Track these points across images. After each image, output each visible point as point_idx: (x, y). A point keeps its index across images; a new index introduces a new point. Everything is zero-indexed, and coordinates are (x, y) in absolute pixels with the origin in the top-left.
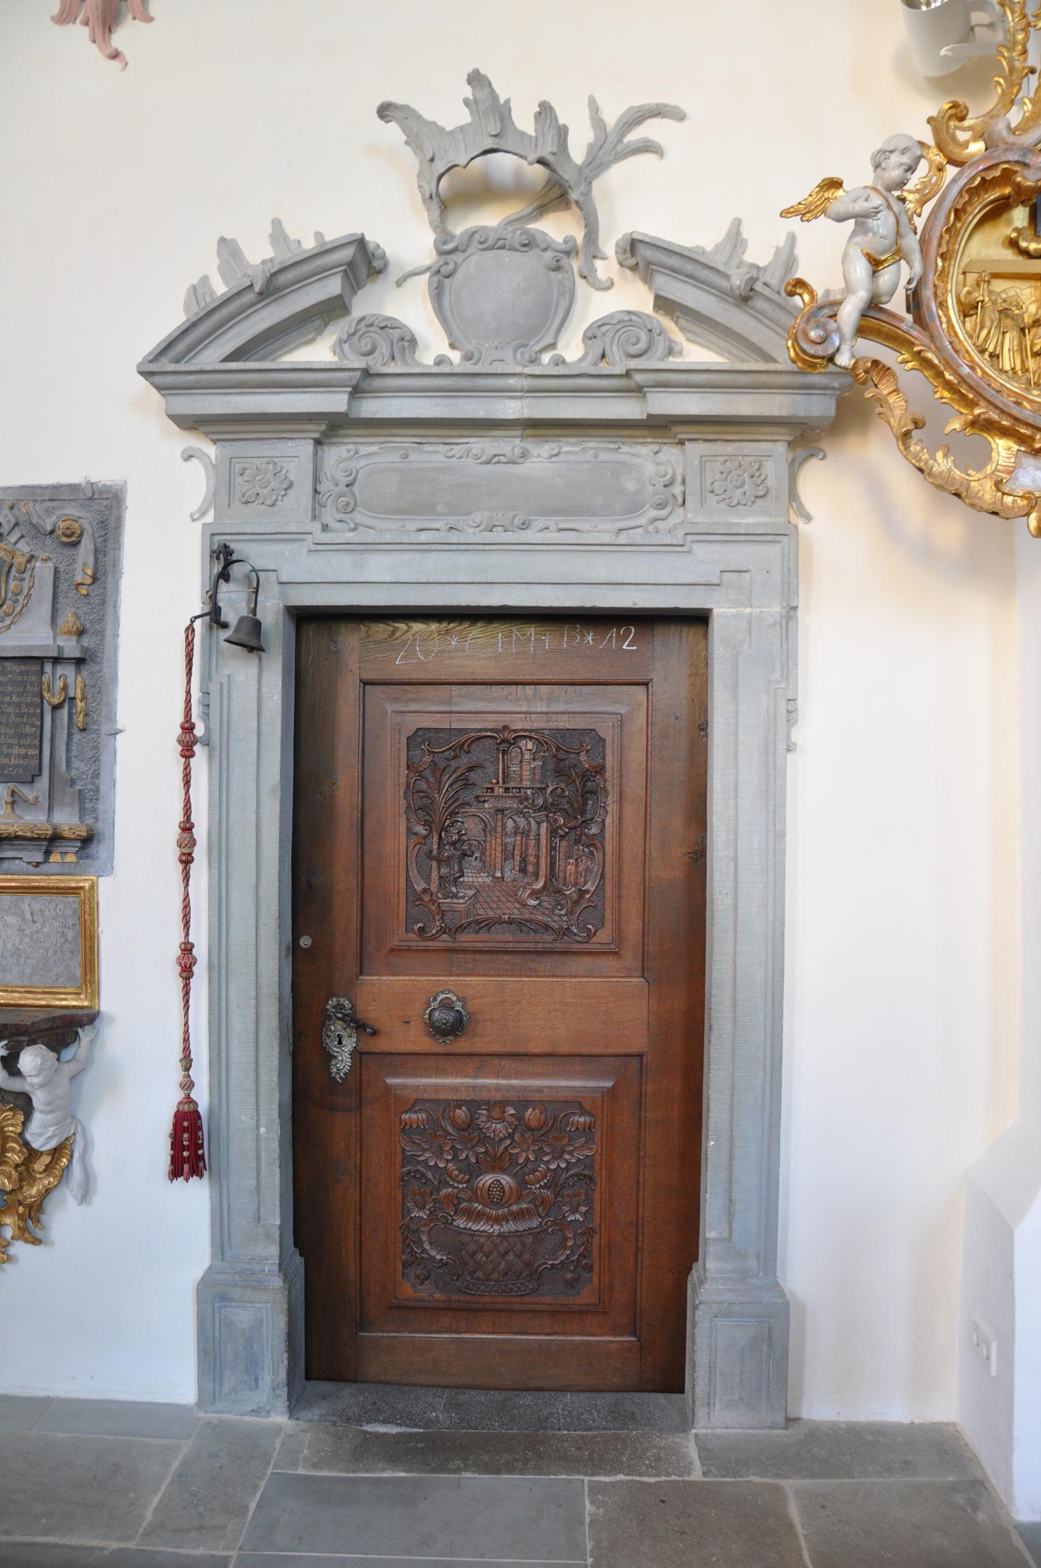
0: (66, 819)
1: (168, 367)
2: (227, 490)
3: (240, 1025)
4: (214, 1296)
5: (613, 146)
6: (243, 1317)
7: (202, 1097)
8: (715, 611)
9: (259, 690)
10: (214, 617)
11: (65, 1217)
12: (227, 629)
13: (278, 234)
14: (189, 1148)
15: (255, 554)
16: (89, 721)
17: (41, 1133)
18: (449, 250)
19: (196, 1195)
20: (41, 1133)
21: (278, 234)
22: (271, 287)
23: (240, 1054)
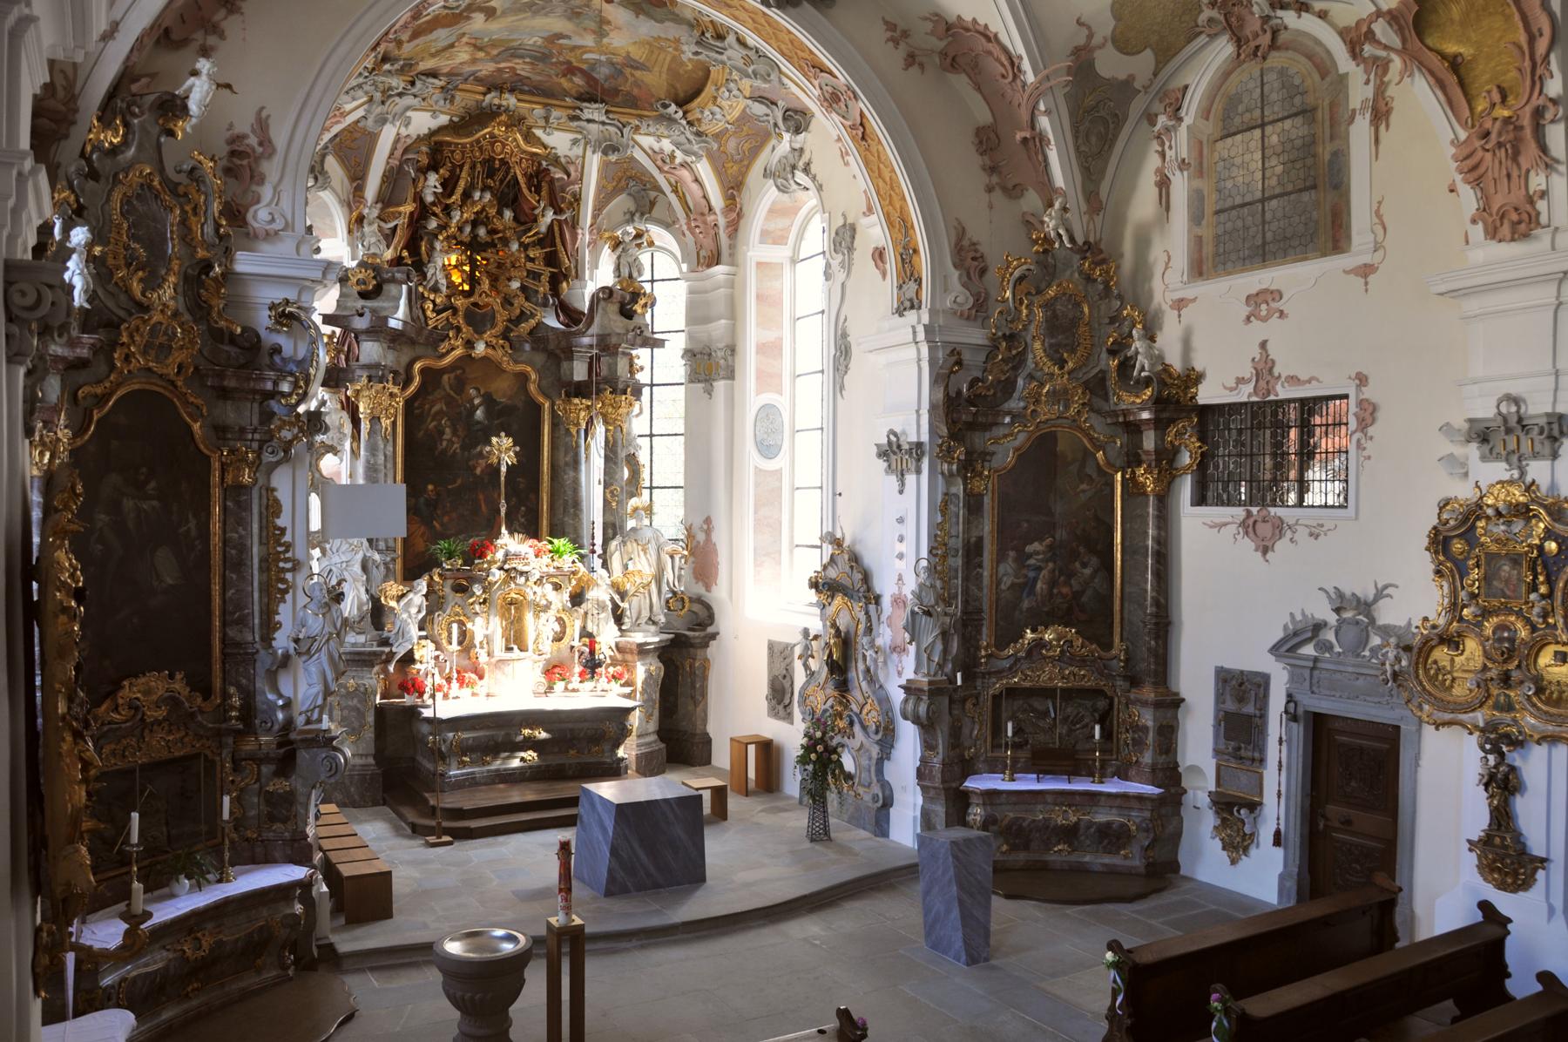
0: (1257, 755)
1: (1275, 650)
2: (1292, 679)
3: (1292, 811)
4: (1282, 878)
5: (1380, 594)
6: (1288, 884)
7: (1282, 828)
8: (1403, 727)
9: (1298, 730)
10: (1286, 712)
11: (1253, 851)
12: (1292, 716)
13: (1303, 614)
14: (1277, 841)
15: (1298, 697)
16: (1262, 731)
17: (1247, 830)
18: (1341, 622)
19: (1279, 853)
20: (1247, 830)
21: (1303, 614)
22: (1295, 634)
23: (1292, 819)
